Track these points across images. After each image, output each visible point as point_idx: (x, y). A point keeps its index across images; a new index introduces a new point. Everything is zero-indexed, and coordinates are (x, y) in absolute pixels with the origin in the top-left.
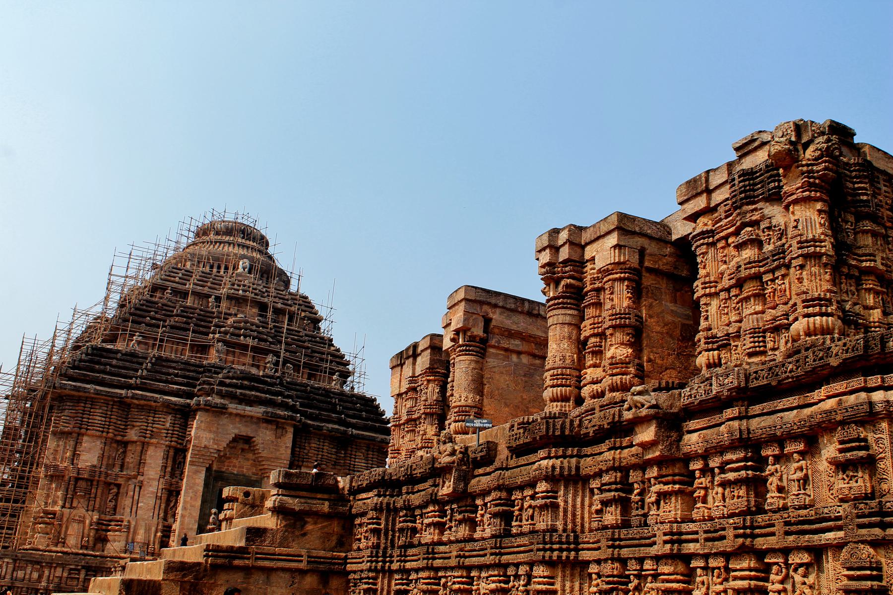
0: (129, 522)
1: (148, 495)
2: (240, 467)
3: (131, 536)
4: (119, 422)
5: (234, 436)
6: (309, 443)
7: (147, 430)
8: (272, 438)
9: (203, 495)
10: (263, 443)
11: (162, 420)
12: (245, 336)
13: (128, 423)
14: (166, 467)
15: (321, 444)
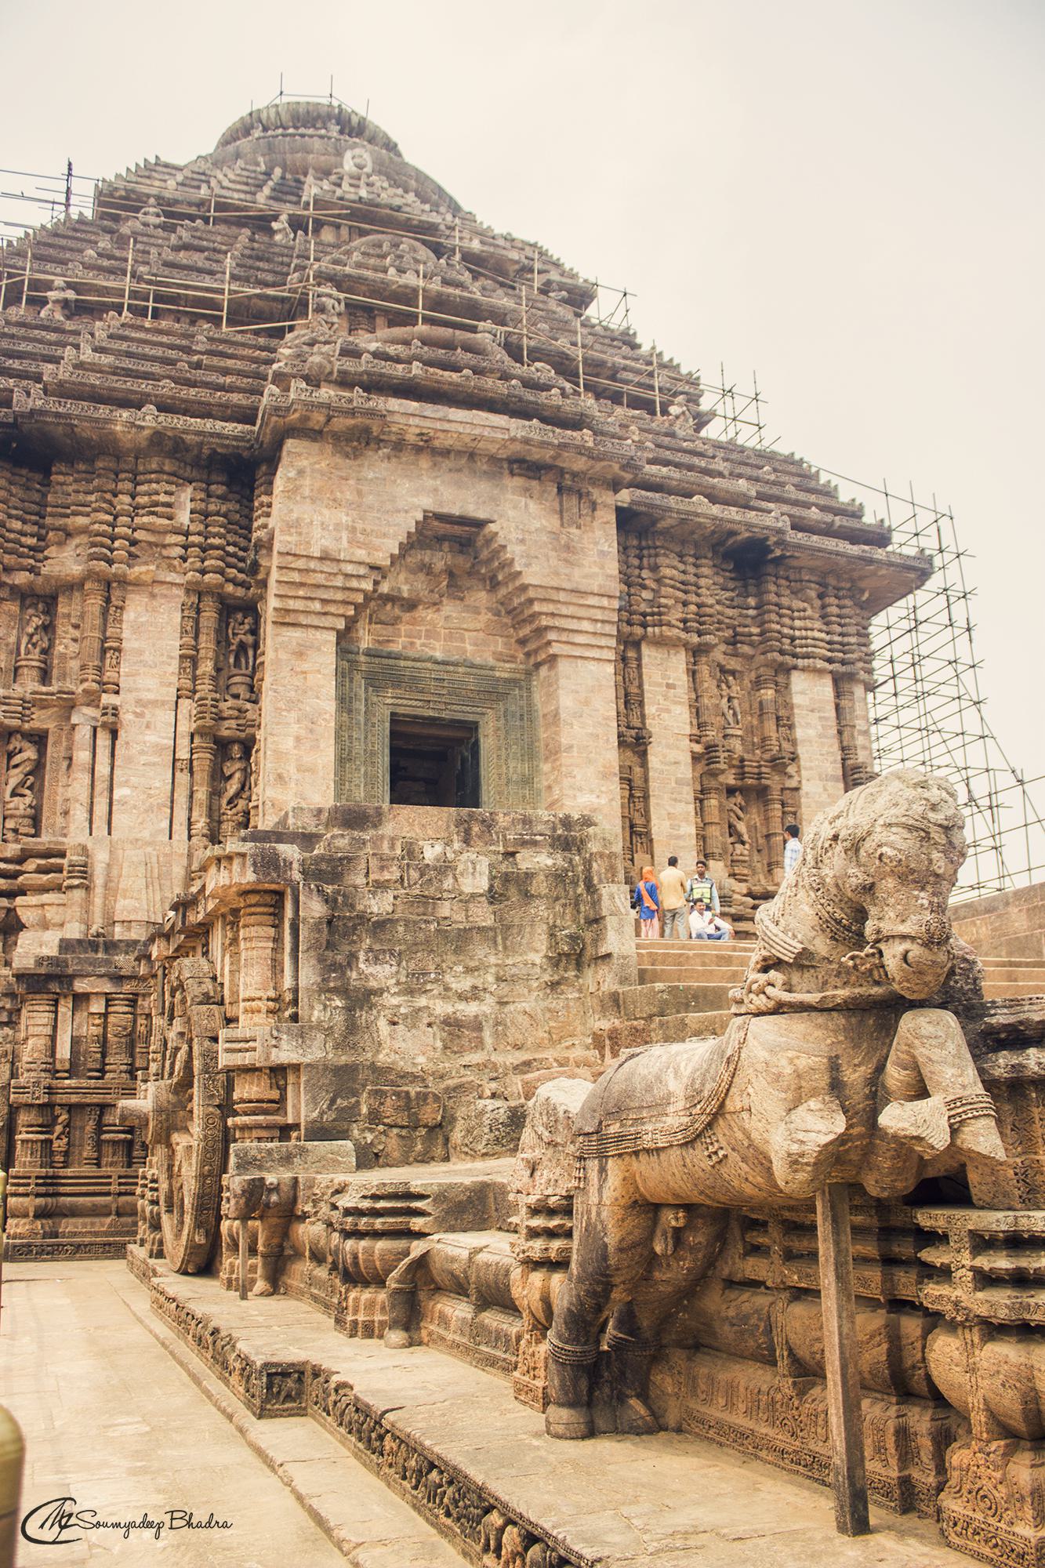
0: (84, 850)
1: (143, 759)
2: (450, 637)
3: (98, 901)
4: (17, 525)
5: (420, 517)
6: (655, 568)
7: (113, 539)
8: (554, 522)
9: (338, 737)
10: (522, 541)
11: (163, 498)
12: (401, 271)
13: (48, 520)
14: (194, 661)
15: (691, 569)
